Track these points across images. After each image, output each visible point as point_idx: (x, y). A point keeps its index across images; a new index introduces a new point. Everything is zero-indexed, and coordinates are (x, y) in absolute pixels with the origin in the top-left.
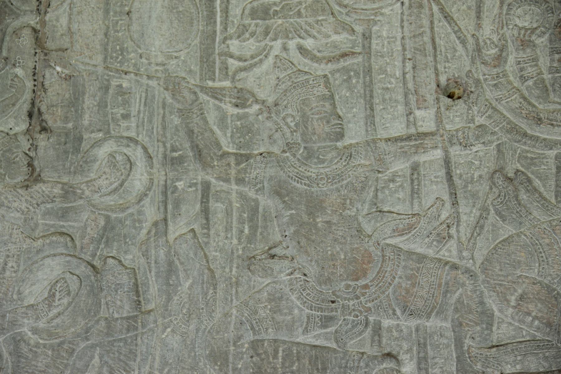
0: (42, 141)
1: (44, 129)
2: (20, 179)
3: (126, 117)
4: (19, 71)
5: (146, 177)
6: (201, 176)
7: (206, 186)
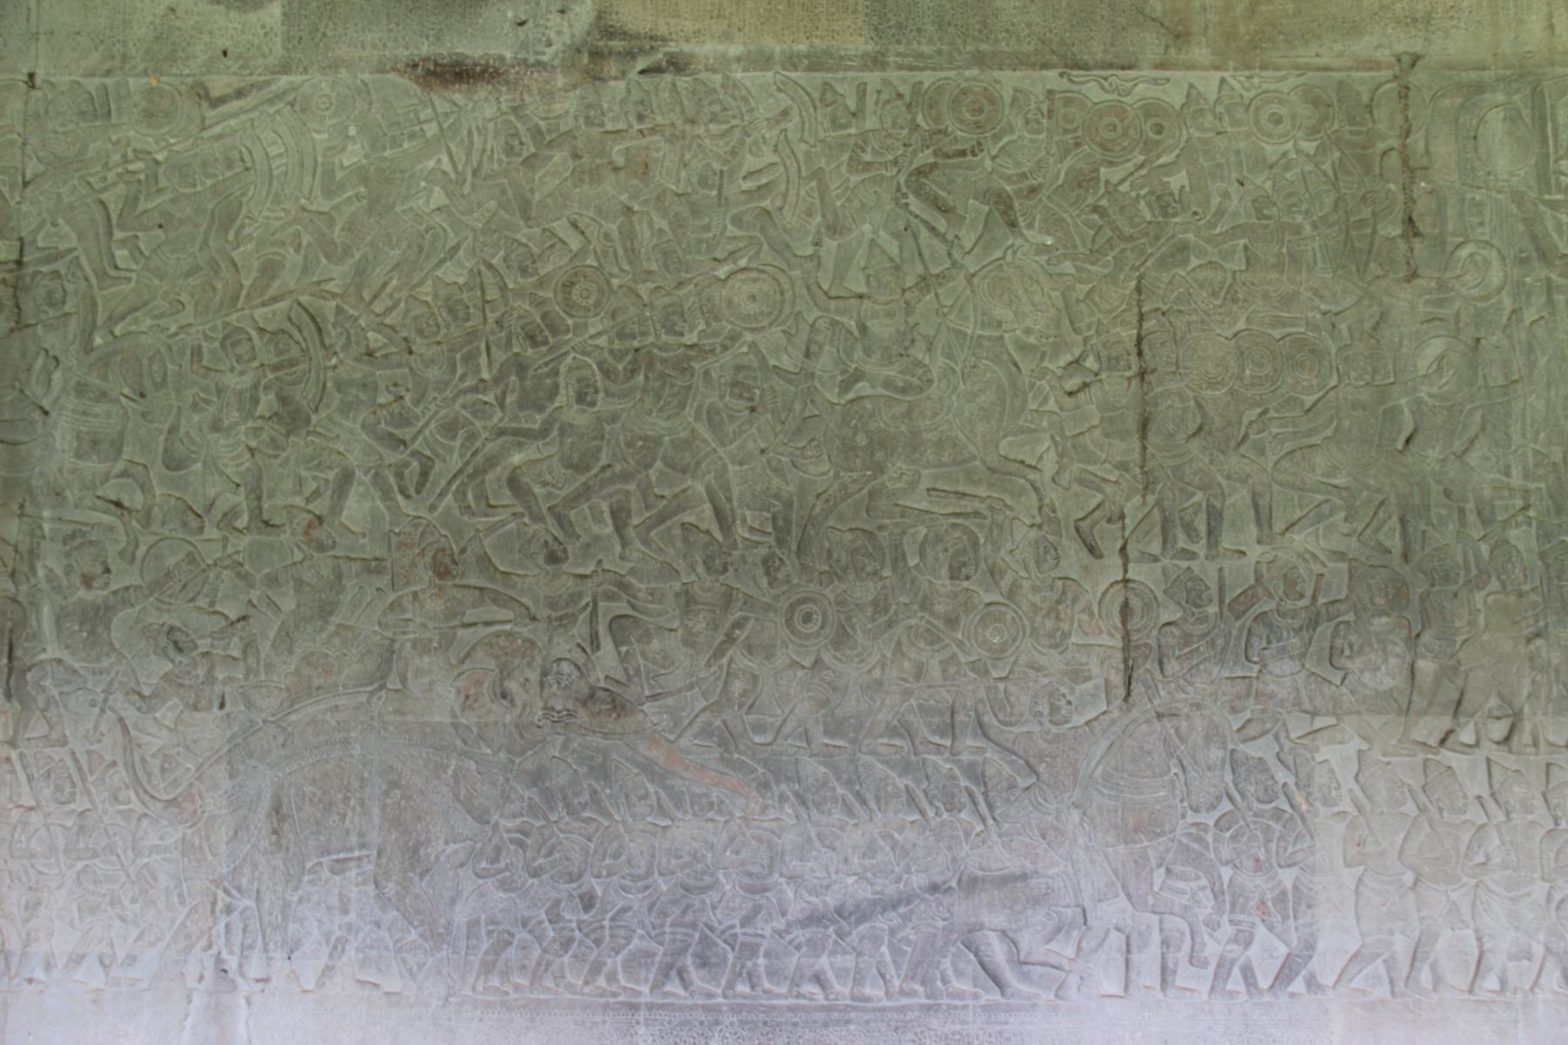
0: (1417, 244)
1: (1416, 234)
2: (1402, 274)
3: (1481, 224)
4: (1392, 186)
5: (1501, 274)
6: (1544, 273)
7: (1549, 280)
